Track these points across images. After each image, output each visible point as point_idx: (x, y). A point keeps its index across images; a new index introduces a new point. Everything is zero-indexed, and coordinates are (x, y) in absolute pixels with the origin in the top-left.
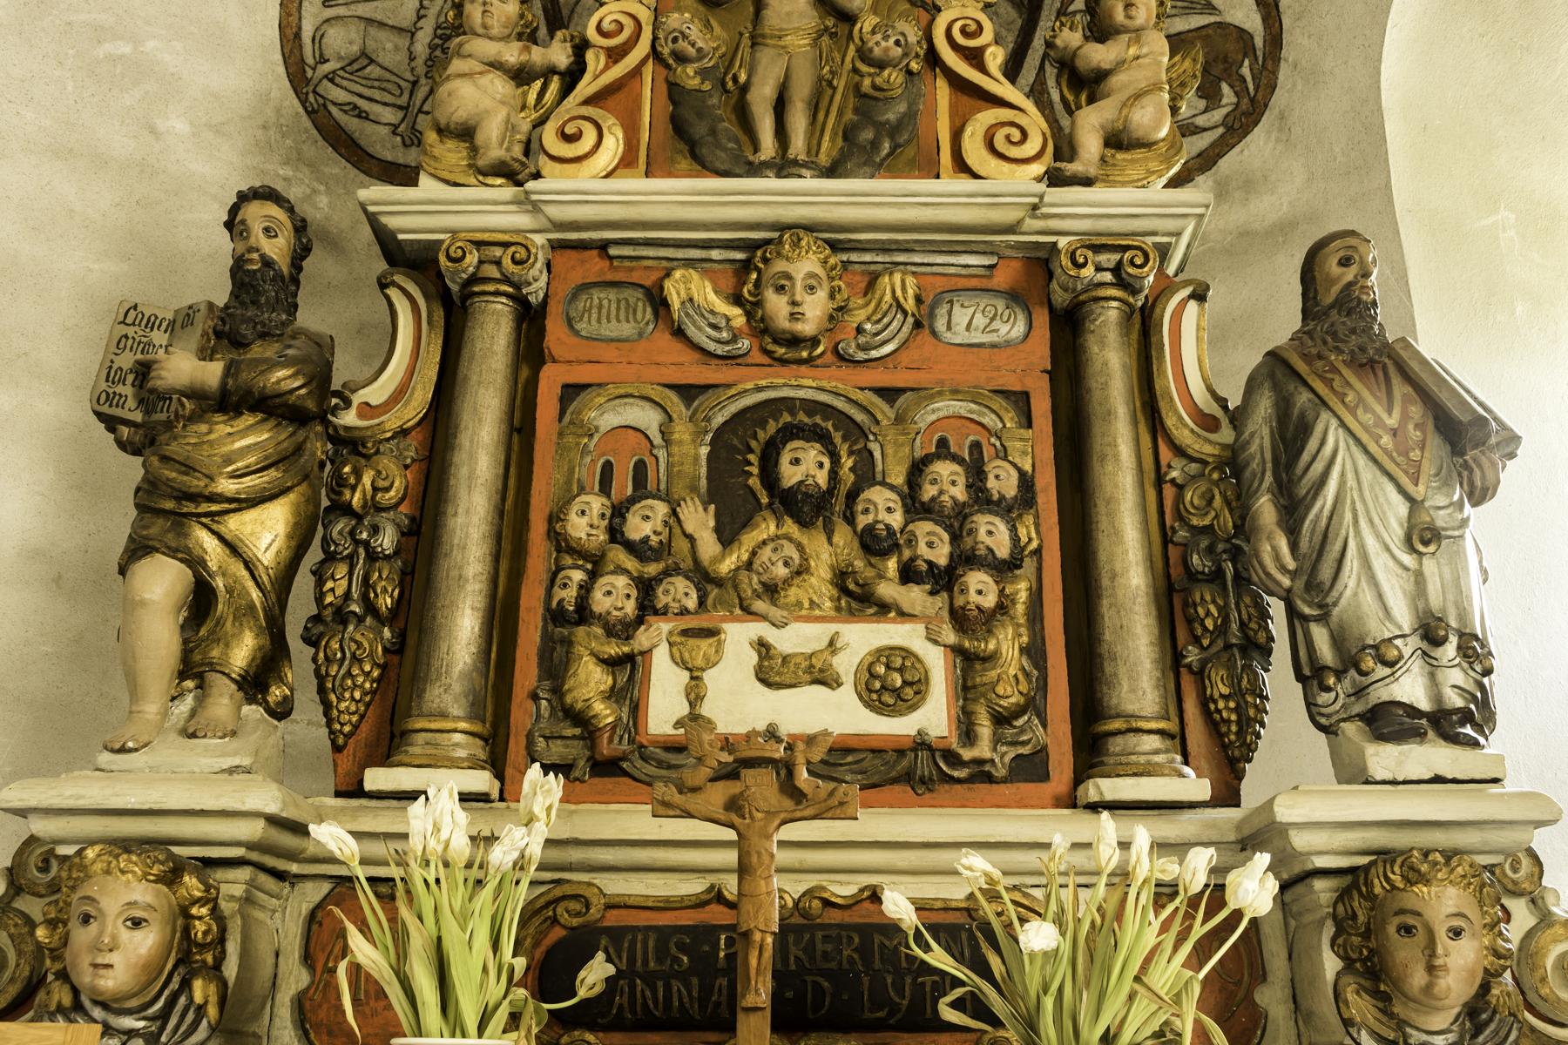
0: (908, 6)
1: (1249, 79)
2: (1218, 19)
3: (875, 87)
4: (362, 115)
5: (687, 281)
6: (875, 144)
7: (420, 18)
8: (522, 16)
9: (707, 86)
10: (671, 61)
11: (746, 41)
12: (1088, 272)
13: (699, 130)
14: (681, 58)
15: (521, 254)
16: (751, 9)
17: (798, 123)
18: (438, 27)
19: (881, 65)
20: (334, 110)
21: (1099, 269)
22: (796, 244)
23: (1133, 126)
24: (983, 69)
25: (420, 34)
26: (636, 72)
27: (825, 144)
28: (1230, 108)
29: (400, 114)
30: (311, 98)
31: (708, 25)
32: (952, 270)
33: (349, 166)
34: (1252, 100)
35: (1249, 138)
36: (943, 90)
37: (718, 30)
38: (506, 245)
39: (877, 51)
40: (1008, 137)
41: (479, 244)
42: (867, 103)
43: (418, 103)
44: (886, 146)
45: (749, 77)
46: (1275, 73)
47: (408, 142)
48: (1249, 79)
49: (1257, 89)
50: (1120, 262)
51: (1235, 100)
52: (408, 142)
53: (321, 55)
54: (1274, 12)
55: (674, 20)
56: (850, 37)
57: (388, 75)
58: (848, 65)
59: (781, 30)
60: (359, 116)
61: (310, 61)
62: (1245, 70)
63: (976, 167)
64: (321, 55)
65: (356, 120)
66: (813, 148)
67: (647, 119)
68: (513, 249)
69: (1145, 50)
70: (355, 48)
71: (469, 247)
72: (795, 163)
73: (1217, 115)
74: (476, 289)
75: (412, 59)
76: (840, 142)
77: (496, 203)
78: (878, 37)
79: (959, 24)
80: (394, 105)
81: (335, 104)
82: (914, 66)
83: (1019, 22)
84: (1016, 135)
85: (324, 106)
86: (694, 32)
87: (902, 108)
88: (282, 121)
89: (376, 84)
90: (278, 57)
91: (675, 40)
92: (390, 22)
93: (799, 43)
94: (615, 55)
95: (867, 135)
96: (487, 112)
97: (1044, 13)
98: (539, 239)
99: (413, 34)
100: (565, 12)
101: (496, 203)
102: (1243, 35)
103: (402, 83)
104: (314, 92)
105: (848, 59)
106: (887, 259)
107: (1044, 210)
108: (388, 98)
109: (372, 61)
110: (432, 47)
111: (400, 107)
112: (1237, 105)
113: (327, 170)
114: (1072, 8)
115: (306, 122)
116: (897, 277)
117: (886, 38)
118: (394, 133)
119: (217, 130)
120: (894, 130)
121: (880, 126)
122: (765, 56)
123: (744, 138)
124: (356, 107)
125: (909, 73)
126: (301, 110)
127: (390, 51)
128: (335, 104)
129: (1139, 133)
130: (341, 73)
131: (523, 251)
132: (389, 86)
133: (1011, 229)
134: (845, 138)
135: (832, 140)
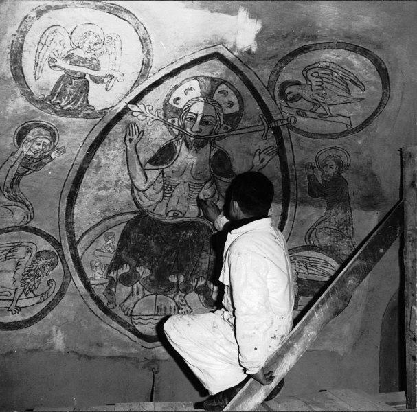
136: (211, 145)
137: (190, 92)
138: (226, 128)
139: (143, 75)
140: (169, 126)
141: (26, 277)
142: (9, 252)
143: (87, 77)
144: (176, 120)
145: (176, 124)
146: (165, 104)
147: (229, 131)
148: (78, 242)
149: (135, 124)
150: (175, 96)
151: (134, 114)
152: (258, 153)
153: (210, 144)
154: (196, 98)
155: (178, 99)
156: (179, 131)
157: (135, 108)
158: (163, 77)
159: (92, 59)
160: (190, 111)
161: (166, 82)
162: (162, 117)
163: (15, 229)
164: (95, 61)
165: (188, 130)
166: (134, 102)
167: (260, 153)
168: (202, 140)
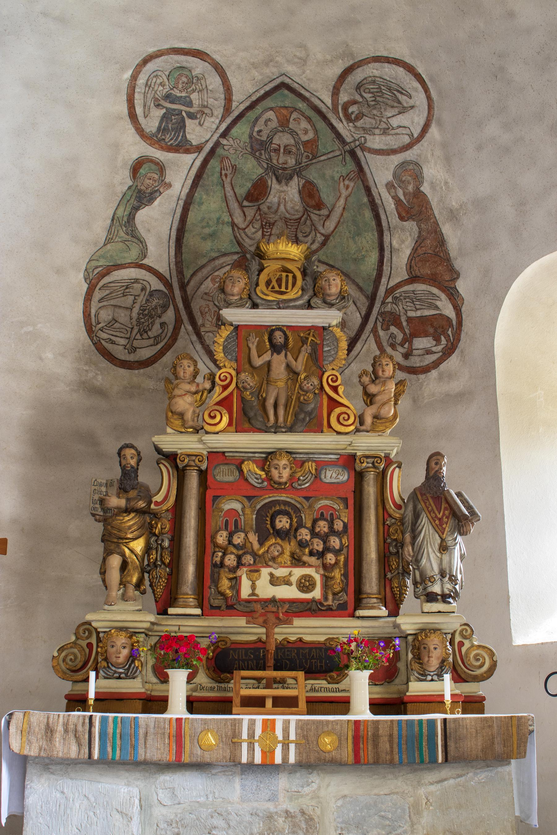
0: (315, 368)
1: (451, 336)
2: (440, 312)
3: (304, 399)
4: (113, 343)
5: (248, 465)
6: (304, 419)
7: (134, 303)
8: (194, 370)
9: (253, 399)
10: (242, 389)
11: (265, 382)
12: (365, 465)
13: (252, 414)
14: (245, 389)
15: (201, 459)
16: (267, 369)
17: (281, 412)
18: (141, 306)
19: (307, 392)
20: (103, 342)
21: (368, 463)
22: (280, 455)
23: (382, 414)
24: (337, 393)
25: (134, 309)
26: (231, 394)
27: (289, 419)
28: (444, 346)
29: (127, 341)
30: (95, 338)
31: (253, 376)
32: (326, 460)
33: (108, 363)
34: (452, 344)
35: (451, 358)
36: (325, 397)
37: (256, 377)
38: (196, 456)
39: (305, 388)
40: (344, 418)
41: (189, 455)
42: (301, 405)
43: (134, 336)
44: (308, 419)
45: (266, 395)
46: (460, 334)
47: (130, 351)
48: (451, 336)
49: (454, 340)
50: (373, 462)
51: (446, 343)
52: (130, 351)
53: (98, 321)
54: (460, 313)
55: (243, 376)
56: (297, 380)
57: (122, 326)
58: (296, 391)
59: (276, 379)
60: (112, 343)
61: (94, 324)
62: (450, 332)
63: (334, 428)
64: (98, 321)
65: (111, 345)
66: (285, 421)
67: (235, 409)
68: (198, 457)
69: (387, 388)
70: (110, 317)
71: (186, 457)
72: (280, 427)
73: (440, 348)
74: (188, 468)
75: (131, 319)
76: (294, 418)
77: (192, 442)
78: (306, 382)
79: (330, 377)
80: (125, 338)
81: (103, 339)
82: (317, 392)
83: (367, 304)
84: (346, 417)
85: (99, 340)
86: (249, 380)
87: (312, 406)
88: (85, 348)
89: (118, 330)
90: (82, 324)
91: (243, 383)
92: (123, 306)
93: (281, 384)
94: (225, 388)
95: (302, 416)
96: (187, 409)
97: (377, 301)
98: (205, 453)
99: (132, 309)
100: (190, 298)
101: (192, 442)
102: (448, 319)
103: (128, 329)
104: (96, 336)
105: (296, 389)
106: (307, 456)
107: (353, 445)
108: (122, 335)
109: (116, 321)
110: (139, 314)
111: (127, 338)
112: (447, 345)
113: (100, 365)
114: (387, 301)
115: (93, 348)
116: (310, 463)
117: (308, 383)
118: (125, 348)
119: (62, 355)
120: (310, 413)
121: (306, 413)
122: (271, 388)
123: (264, 416)
124: (111, 340)
125: (315, 394)
126: (91, 343)
127: (123, 316)
128: (103, 339)
129: (384, 416)
130: (105, 327)
131: (201, 458)
132: (123, 330)
133: (345, 449)
134: (295, 417)
135: (291, 417)
136: (298, 176)
137: (269, 123)
138: (307, 157)
139: (227, 109)
140: (258, 159)
141: (141, 316)
142: (127, 288)
143: (184, 114)
144: (263, 152)
145: (263, 157)
146: (251, 137)
147: (311, 160)
148: (189, 282)
149: (227, 158)
150: (256, 129)
151: (226, 147)
152: (341, 179)
153: (297, 175)
154: (275, 128)
155: (260, 131)
156: (267, 163)
157: (224, 142)
158: (243, 110)
159: (186, 97)
160: (273, 142)
161: (248, 114)
162: (249, 150)
163: (132, 265)
164: (188, 99)
165: (275, 161)
166: (224, 135)
167: (344, 180)
168: (290, 172)
